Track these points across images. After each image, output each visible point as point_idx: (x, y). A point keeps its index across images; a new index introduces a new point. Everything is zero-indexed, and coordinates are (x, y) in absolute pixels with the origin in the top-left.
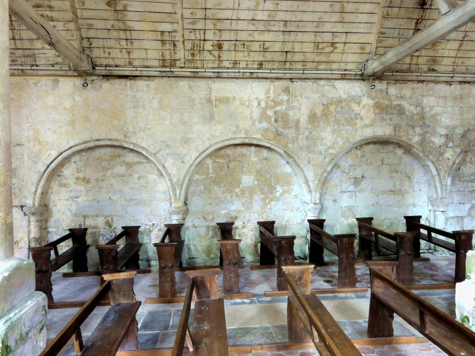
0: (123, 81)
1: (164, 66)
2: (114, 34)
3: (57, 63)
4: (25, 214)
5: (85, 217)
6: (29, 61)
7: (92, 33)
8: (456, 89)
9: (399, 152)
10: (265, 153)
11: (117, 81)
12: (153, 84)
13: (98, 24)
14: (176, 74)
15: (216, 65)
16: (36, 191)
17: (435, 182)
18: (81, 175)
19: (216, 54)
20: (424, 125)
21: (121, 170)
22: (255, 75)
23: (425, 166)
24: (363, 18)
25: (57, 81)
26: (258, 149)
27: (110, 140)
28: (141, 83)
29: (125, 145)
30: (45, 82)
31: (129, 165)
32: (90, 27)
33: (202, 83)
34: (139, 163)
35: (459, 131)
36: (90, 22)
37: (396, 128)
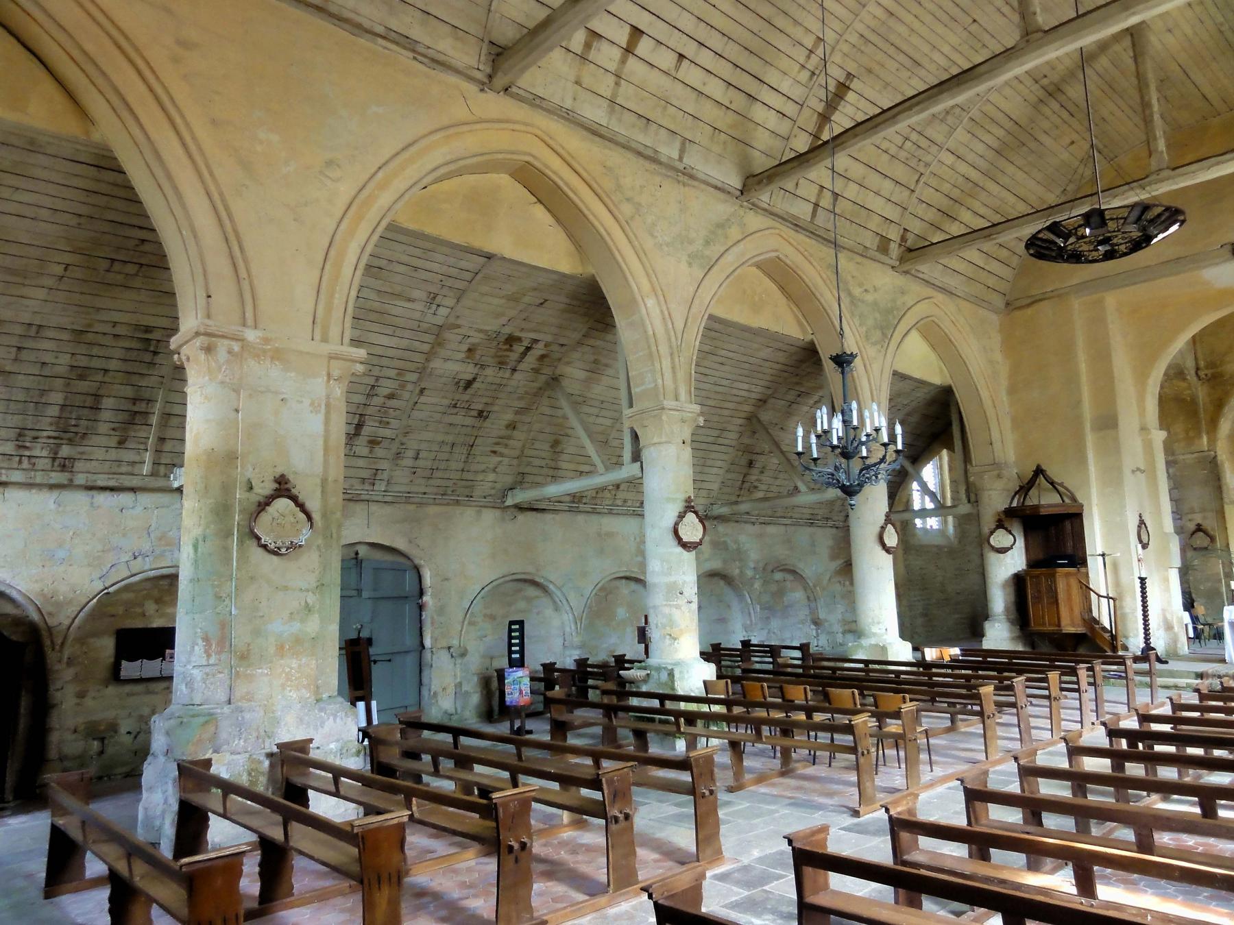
0: (534, 513)
1: (574, 502)
2: (545, 471)
3: (490, 495)
4: (452, 656)
5: (492, 658)
6: (467, 492)
7: (527, 470)
8: (757, 528)
9: (722, 583)
10: (633, 585)
11: (530, 514)
12: (558, 517)
13: (537, 462)
14: (581, 509)
15: (610, 503)
16: (461, 631)
17: (749, 609)
18: (488, 612)
19: (613, 492)
20: (741, 560)
21: (522, 605)
22: (636, 513)
23: (741, 597)
24: (715, 471)
25: (479, 512)
26: (628, 581)
27: (524, 573)
28: (548, 517)
29: (537, 579)
30: (470, 512)
31: (529, 600)
32: (529, 464)
33: (594, 517)
34: (537, 597)
35: (761, 565)
36: (531, 459)
37: (725, 562)
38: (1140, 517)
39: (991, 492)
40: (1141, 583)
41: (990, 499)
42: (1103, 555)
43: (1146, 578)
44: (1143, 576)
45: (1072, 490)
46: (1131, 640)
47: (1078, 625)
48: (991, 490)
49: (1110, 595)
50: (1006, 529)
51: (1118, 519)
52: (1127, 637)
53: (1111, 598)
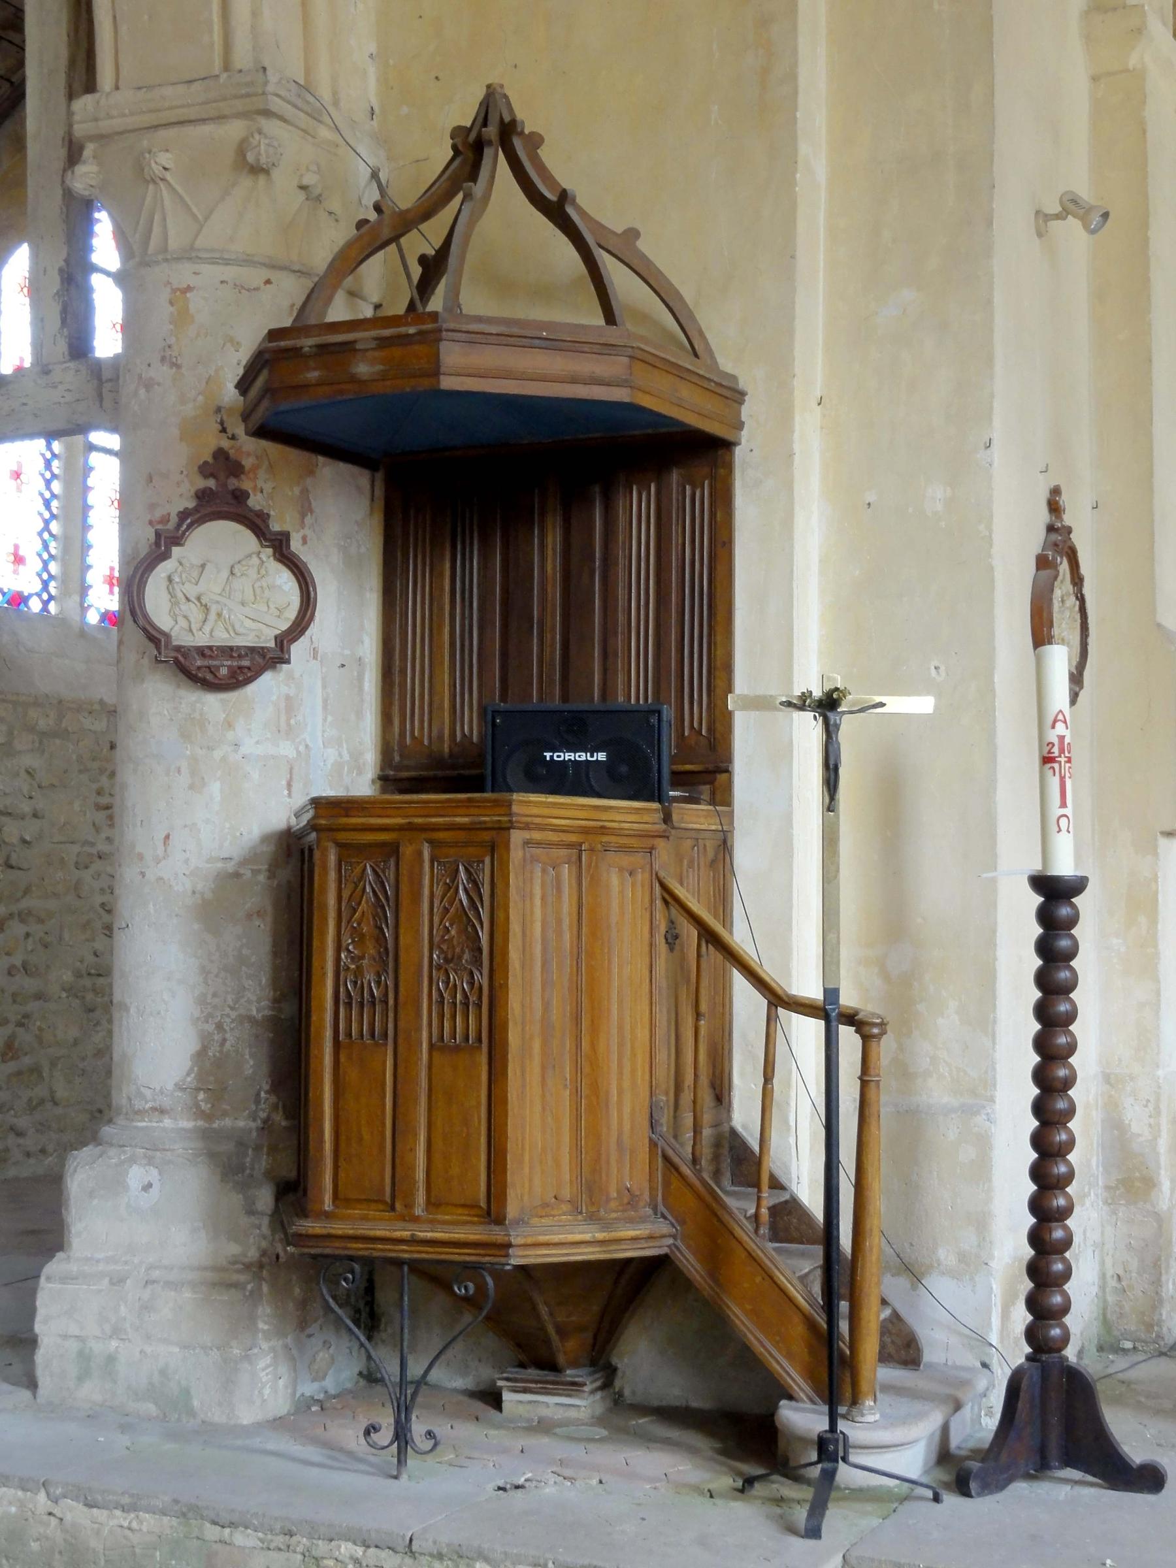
38: (1054, 507)
39: (183, 274)
40: (1045, 916)
41: (182, 318)
42: (828, 705)
43: (1076, 886)
44: (1064, 867)
45: (688, 293)
46: (940, 1286)
47: (631, 1200)
48: (189, 254)
49: (848, 999)
50: (257, 524)
51: (936, 495)
52: (913, 1272)
53: (850, 1019)
